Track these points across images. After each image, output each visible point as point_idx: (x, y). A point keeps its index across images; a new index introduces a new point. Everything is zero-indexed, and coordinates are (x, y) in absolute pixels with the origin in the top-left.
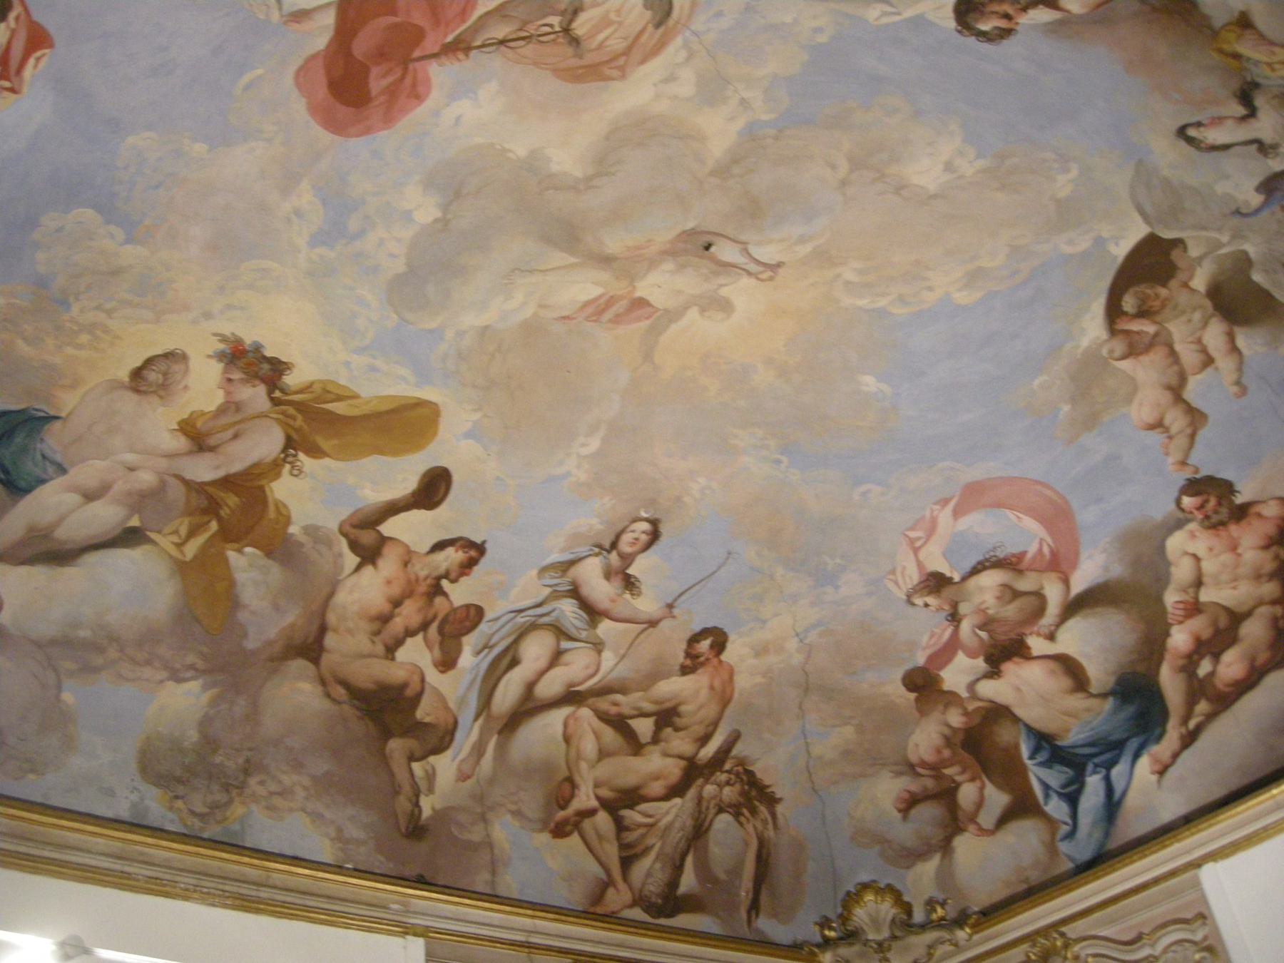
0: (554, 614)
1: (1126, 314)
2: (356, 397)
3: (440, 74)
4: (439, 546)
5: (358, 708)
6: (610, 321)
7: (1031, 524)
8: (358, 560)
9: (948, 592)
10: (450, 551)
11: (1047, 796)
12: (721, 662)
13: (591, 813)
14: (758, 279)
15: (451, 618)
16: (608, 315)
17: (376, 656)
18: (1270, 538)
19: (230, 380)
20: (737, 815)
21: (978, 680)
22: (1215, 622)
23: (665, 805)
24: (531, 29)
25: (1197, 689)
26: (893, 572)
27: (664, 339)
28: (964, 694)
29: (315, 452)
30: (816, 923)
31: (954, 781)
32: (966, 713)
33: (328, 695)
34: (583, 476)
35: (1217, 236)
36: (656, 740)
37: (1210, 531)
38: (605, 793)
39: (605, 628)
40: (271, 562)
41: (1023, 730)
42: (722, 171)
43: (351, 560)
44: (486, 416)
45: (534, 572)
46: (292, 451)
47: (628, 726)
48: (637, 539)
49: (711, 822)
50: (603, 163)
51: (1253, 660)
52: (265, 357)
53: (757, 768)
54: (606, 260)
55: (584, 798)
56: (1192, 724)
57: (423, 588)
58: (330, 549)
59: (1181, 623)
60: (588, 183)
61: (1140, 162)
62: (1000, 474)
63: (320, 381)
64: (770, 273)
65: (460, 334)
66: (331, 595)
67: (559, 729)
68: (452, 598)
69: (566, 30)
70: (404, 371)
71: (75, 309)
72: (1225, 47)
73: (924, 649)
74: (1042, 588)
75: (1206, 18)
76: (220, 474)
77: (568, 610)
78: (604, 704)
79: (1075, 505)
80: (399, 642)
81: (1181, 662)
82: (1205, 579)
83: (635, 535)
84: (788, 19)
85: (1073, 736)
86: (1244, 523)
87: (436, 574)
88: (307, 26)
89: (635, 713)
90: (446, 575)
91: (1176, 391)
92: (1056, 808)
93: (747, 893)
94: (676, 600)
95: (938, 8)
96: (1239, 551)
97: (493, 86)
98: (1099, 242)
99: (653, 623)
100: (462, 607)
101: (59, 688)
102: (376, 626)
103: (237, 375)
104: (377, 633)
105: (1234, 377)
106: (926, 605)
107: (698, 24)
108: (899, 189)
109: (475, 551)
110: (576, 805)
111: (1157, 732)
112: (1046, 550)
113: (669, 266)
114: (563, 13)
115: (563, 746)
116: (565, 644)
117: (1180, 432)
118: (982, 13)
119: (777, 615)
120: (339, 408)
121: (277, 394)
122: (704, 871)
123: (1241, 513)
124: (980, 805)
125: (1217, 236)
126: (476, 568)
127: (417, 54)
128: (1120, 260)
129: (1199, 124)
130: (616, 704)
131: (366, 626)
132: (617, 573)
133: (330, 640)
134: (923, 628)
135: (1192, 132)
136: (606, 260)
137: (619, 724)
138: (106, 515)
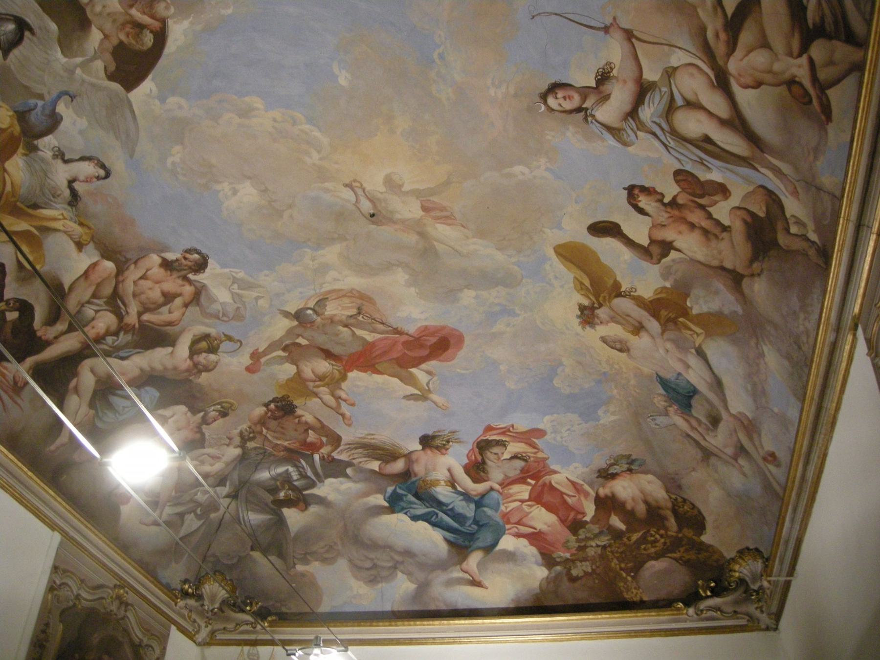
1: (151, 32)
2: (575, 278)
3: (412, 329)
4: (641, 211)
5: (764, 258)
6: (447, 211)
8: (672, 252)
10: (641, 205)
14: (362, 185)
16: (444, 214)
17: (731, 236)
24: (370, 321)
27: (432, 185)
29: (617, 285)
33: (759, 275)
34: (543, 161)
35: (84, 76)
38: (796, 44)
39: (651, 74)
42: (342, 238)
43: (673, 255)
45: (630, 149)
47: (734, 15)
48: (565, 98)
50: (388, 267)
54: (422, 235)
57: (676, 212)
58: (671, 267)
60: (400, 264)
61: (131, 157)
64: (354, 184)
68: (675, 193)
70: (547, 267)
75: (97, 248)
76: (651, 319)
77: (648, 113)
78: (720, 48)
80: (718, 223)
83: (562, 101)
87: (663, 208)
88: (432, 369)
89: (719, 10)
90: (661, 201)
94: (598, 29)
98: (163, 100)
99: (629, 35)
103: (597, 321)
104: (716, 237)
107: (312, 292)
109: (633, 192)
113: (397, 216)
115: (763, 87)
116: (679, 102)
118: (196, 262)
120: (587, 282)
121: (596, 305)
125: (84, 76)
126: (647, 186)
128: (150, 77)
129: (98, 178)
130: (717, 36)
131: (714, 243)
132: (600, 92)
133: (728, 265)
135: (102, 173)
136: (422, 235)
138: (693, 360)
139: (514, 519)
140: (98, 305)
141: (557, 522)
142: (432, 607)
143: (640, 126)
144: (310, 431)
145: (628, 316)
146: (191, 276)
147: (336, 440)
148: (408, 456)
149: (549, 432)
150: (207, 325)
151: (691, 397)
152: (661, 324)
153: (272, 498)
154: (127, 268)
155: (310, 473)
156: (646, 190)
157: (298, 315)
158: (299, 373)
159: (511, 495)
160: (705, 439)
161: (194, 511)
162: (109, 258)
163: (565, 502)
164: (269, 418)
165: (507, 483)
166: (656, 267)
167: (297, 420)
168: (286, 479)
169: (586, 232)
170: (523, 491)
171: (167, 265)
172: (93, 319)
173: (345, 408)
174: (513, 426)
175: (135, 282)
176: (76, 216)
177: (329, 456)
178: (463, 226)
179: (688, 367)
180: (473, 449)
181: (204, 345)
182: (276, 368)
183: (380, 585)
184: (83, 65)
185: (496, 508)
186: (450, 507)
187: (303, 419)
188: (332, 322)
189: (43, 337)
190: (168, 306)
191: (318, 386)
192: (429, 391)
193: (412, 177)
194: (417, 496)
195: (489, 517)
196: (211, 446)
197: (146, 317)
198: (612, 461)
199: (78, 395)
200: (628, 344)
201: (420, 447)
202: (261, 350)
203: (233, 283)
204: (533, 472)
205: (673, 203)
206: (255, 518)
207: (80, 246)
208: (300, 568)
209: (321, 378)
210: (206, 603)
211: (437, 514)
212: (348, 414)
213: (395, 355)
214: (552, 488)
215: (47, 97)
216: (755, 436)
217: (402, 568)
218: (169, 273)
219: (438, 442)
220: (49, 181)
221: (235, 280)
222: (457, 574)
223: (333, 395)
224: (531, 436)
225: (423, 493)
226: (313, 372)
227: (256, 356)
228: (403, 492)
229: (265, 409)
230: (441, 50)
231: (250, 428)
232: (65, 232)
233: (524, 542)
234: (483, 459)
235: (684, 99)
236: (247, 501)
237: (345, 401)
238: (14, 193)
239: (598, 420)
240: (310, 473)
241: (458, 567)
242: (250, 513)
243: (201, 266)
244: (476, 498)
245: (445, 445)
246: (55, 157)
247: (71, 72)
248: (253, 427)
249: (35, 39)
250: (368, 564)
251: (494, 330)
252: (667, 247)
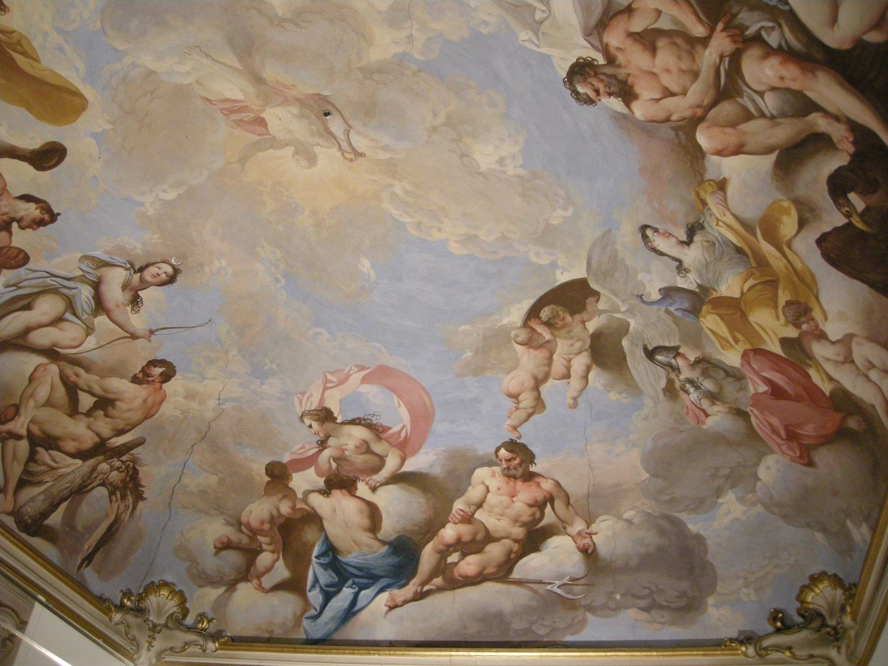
0: (74, 291)
1: (540, 318)
2: (37, 60)
6: (235, 121)
7: (404, 412)
9: (328, 426)
10: (33, 206)
11: (313, 586)
12: (161, 387)
13: (19, 437)
14: (343, 154)
15: (4, 251)
16: (235, 117)
18: (536, 502)
20: (112, 493)
21: (313, 491)
22: (475, 534)
23: (70, 460)
25: (441, 568)
26: (303, 393)
28: (300, 496)
30: (121, 591)
31: (261, 547)
32: (293, 508)
34: (151, 212)
35: (620, 304)
36: (89, 414)
37: (506, 478)
38: (35, 429)
39: (101, 320)
41: (323, 535)
42: (368, 72)
44: (114, 130)
45: (79, 255)
47: (77, 394)
48: (159, 275)
49: (93, 488)
51: (484, 568)
53: (143, 471)
54: (258, 80)
55: (19, 425)
56: (426, 588)
59: (455, 523)
60: (281, 22)
61: (609, 231)
62: (406, 371)
63: (20, 34)
64: (352, 156)
65: (134, 65)
67: (31, 371)
68: (13, 238)
70: (80, 65)
72: (702, 193)
73: (292, 453)
74: (387, 456)
75: (704, 168)
77: (85, 293)
78: (70, 370)
79: (438, 416)
81: (441, 547)
82: (484, 505)
83: (160, 272)
84: (473, 5)
85: (351, 558)
86: (526, 484)
87: (12, 215)
89: (87, 388)
90: (19, 221)
91: (538, 383)
92: (315, 597)
93: (89, 548)
94: (157, 330)
95: (562, 59)
96: (514, 499)
98: (554, 265)
99: (134, 336)
100: (16, 248)
105: (575, 394)
106: (310, 426)
109: (48, 216)
110: (10, 426)
111: (403, 582)
112: (403, 434)
113: (295, 110)
115: (27, 382)
116: (68, 316)
117: (525, 408)
118: (585, 80)
119: (214, 379)
120: (20, 60)
122: (70, 516)
123: (529, 477)
124: (268, 570)
125: (620, 304)
126: (42, 228)
128: (558, 284)
129: (656, 230)
130: (77, 375)
132: (131, 289)
134: (299, 440)
135: (649, 232)
136: (258, 80)
137: (72, 390)
140: (753, 101)
143: (84, 279)
146: (601, 60)
154: (683, 119)
156: (39, 223)
162: (699, 147)
171: (627, 94)
172: (773, 89)
175: (684, 93)
176: (704, 214)
184: (618, 311)
189: (851, 139)
193: (285, 160)
197: (699, 31)
203: (541, 22)
207: (722, 185)
215: (663, 309)
220: (708, 259)
221: (536, 27)
230: (279, 285)
235: (67, 320)
238: (750, 275)
243: (580, 70)
246: (687, 271)
247: (630, 311)
249: (646, 343)
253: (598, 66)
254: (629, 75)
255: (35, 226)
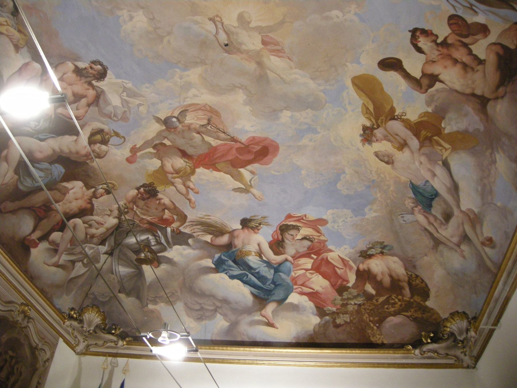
2: (364, 104)
3: (244, 138)
4: (419, 50)
10: (420, 45)
14: (221, 20)
15: (458, 32)
16: (277, 48)
17: (484, 68)
19: (377, 140)
24: (215, 130)
27: (271, 24)
33: (502, 97)
34: (353, 7)
40: (446, 117)
42: (203, 63)
46: (396, 117)
50: (232, 88)
52: (364, 133)
54: (260, 64)
57: (445, 51)
58: (434, 95)
64: (216, 19)
65: (319, 85)
66: (456, 91)
68: (446, 35)
69: (209, 124)
70: (345, 94)
71: (374, 178)
72: (23, 37)
76: (414, 137)
80: (476, 58)
87: (435, 47)
88: (254, 170)
90: (435, 41)
97: (237, 126)
100: (451, 28)
101: (496, 205)
102: (469, 70)
103: (374, 139)
104: (473, 69)
107: (178, 104)
108: (152, 19)
109: (416, 33)
113: (244, 47)
114: (206, 127)
120: (371, 108)
121: (375, 126)
126: (426, 29)
127: (243, 146)
131: (470, 75)
133: (478, 92)
136: (260, 64)
138: (439, 171)
139: (300, 282)
141: (329, 286)
142: (239, 339)
144: (166, 211)
145: (397, 135)
146: (94, 82)
147: (183, 218)
148: (232, 233)
149: (330, 222)
150: (103, 123)
151: (433, 199)
152: (420, 142)
153: (136, 257)
155: (163, 241)
156: (425, 33)
157: (166, 122)
158: (162, 167)
159: (299, 265)
160: (438, 231)
161: (82, 261)
163: (336, 273)
164: (139, 198)
165: (297, 257)
166: (423, 96)
167: (158, 202)
168: (147, 244)
169: (377, 67)
170: (308, 263)
173: (192, 195)
174: (305, 216)
176: (17, 24)
177: (177, 229)
178: (289, 58)
179: (434, 175)
180: (276, 231)
181: (98, 137)
182: (147, 161)
183: (204, 322)
185: (288, 273)
186: (257, 271)
187: (162, 201)
188: (189, 129)
190: (76, 104)
191: (174, 178)
192: (251, 186)
193: (258, 18)
194: (235, 261)
195: (283, 279)
196: (97, 215)
198: (371, 246)
199: (7, 163)
200: (393, 158)
201: (240, 227)
202: (138, 146)
203: (123, 91)
204: (316, 249)
205: (444, 44)
206: (123, 270)
208: (151, 307)
209: (177, 172)
210: (85, 326)
211: (247, 275)
212: (193, 199)
213: (230, 158)
214: (328, 262)
216: (478, 227)
217: (220, 311)
218: (79, 78)
219: (253, 224)
221: (125, 89)
222: (257, 317)
223: (184, 185)
224: (317, 224)
225: (239, 261)
226: (172, 167)
227: (134, 150)
228: (226, 259)
229: (136, 191)
231: (125, 204)
232: (7, 36)
233: (305, 298)
234: (282, 238)
236: (119, 258)
237: (192, 189)
239: (364, 215)
240: (163, 241)
241: (259, 312)
242: (120, 267)
243: (102, 75)
244: (275, 266)
245: (257, 226)
248: (128, 204)
250: (197, 307)
251: (301, 143)
252: (434, 79)
253: (94, 80)
254: (80, 80)
255: (429, 32)
